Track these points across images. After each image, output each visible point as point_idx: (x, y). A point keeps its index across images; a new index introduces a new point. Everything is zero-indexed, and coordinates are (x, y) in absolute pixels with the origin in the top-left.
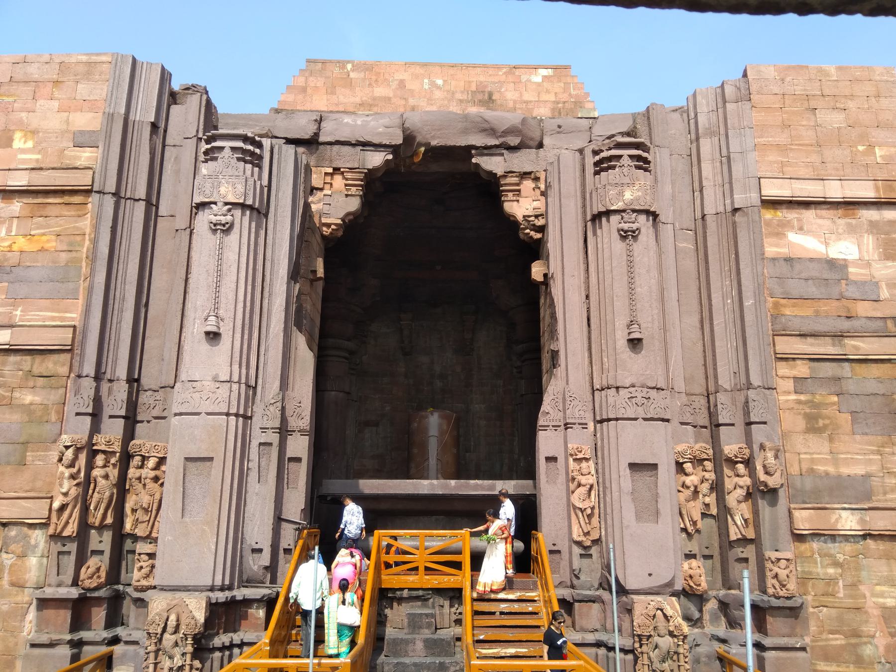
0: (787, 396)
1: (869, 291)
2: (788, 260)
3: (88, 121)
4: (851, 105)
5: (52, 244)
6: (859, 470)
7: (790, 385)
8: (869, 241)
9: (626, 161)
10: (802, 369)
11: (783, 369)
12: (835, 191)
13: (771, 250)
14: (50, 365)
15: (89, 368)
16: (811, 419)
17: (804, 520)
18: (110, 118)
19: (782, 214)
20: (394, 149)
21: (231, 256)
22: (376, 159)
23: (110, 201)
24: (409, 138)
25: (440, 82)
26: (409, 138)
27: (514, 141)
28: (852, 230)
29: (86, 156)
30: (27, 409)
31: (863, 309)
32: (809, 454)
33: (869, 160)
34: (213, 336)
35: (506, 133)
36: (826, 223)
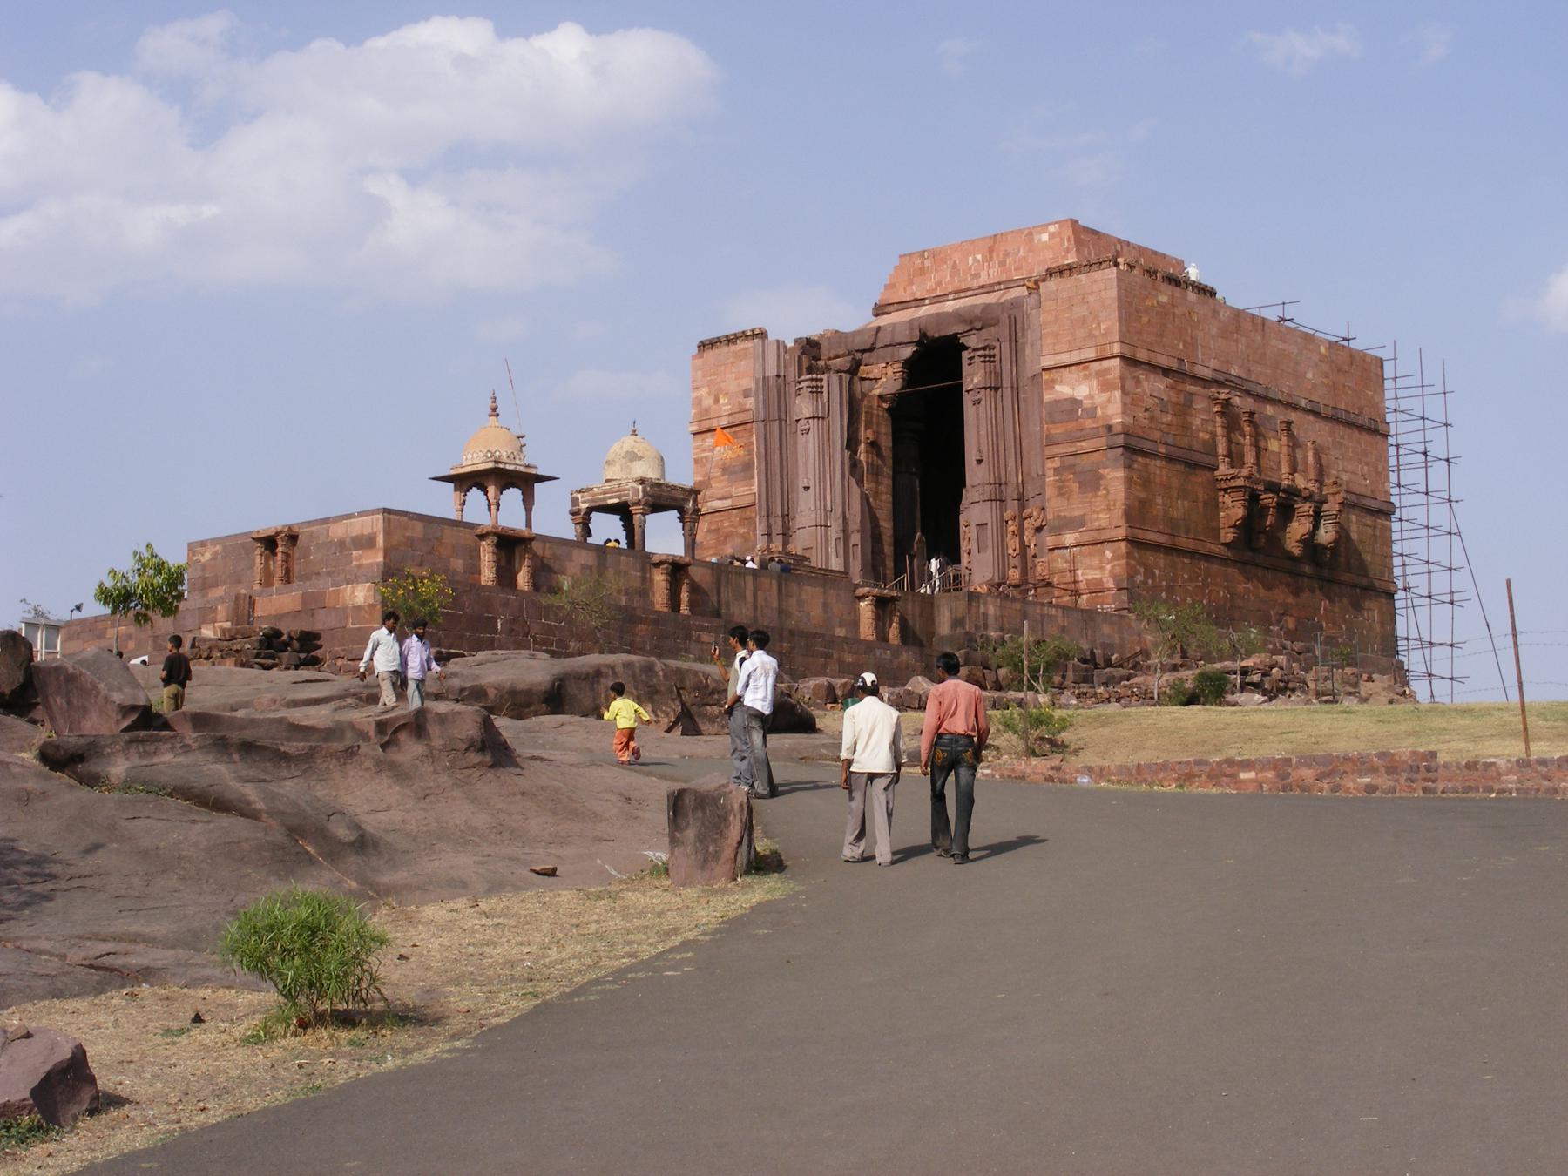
0: (1050, 479)
1: (1091, 412)
2: (1057, 401)
3: (748, 383)
4: (1091, 299)
5: (742, 452)
6: (1077, 513)
7: (1050, 472)
8: (1095, 382)
9: (977, 360)
10: (1057, 463)
11: (1049, 464)
12: (1076, 357)
13: (1047, 397)
14: (748, 513)
15: (764, 513)
16: (1060, 488)
17: (1050, 541)
18: (757, 382)
19: (1054, 374)
20: (918, 343)
21: (811, 446)
22: (907, 352)
23: (761, 425)
24: (923, 335)
25: (979, 257)
26: (923, 335)
27: (978, 325)
28: (1086, 377)
29: (750, 402)
30: (743, 536)
31: (1089, 423)
32: (1056, 506)
33: (1096, 333)
34: (806, 488)
35: (971, 322)
36: (1074, 376)
